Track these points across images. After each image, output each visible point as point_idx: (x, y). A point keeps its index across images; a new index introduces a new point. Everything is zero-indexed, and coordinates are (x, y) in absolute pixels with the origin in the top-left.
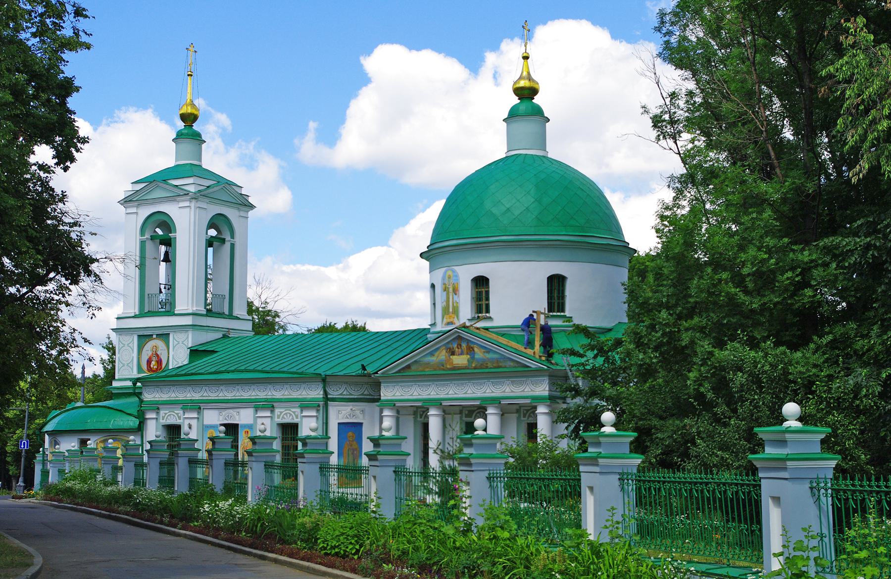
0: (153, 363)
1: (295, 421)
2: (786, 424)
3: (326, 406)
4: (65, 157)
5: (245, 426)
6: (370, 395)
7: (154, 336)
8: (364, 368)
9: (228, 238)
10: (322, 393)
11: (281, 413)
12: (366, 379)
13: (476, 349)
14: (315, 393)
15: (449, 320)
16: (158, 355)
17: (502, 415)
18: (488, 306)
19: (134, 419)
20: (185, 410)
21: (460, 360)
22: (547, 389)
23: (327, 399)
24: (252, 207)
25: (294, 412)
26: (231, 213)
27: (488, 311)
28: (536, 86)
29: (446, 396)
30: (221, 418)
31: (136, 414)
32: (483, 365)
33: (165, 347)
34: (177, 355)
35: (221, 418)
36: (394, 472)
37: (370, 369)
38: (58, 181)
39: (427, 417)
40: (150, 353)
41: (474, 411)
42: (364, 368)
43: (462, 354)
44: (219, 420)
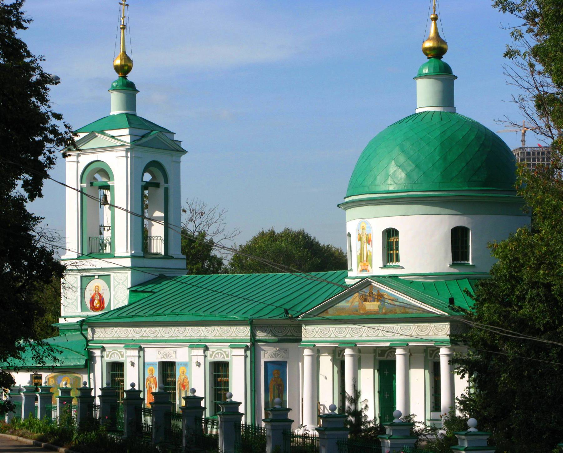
0: (96, 302)
1: (226, 359)
2: (469, 430)
4: (34, 190)
5: (181, 364)
7: (96, 277)
9: (162, 182)
11: (213, 352)
12: (289, 322)
15: (363, 268)
17: (411, 355)
18: (397, 255)
20: (126, 347)
21: (372, 306)
23: (254, 340)
24: (184, 152)
25: (225, 352)
26: (164, 158)
27: (398, 260)
28: (444, 46)
29: (360, 339)
30: (160, 356)
33: (107, 287)
34: (118, 293)
35: (160, 356)
36: (283, 433)
38: (31, 207)
39: (344, 356)
40: (93, 293)
41: (387, 350)
42: (286, 311)
44: (158, 358)
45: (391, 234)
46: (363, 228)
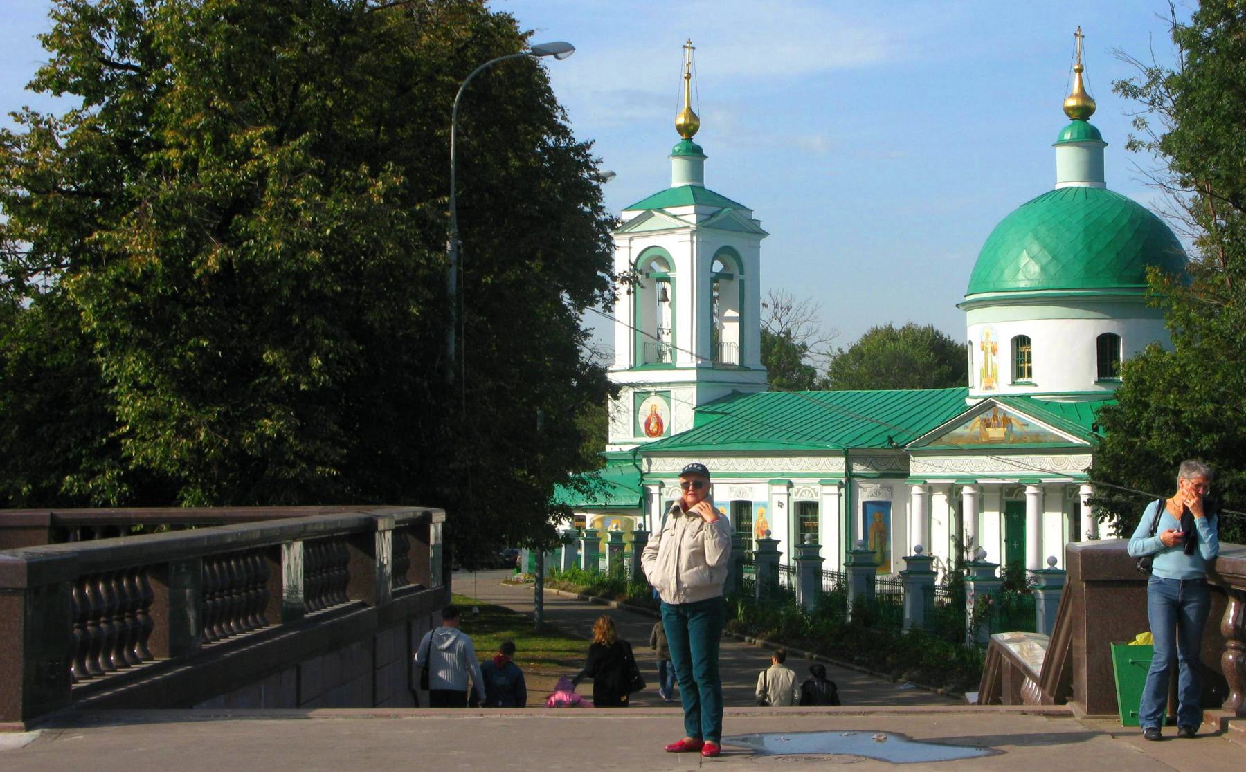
0: (653, 425)
1: (815, 499)
8: (890, 440)
12: (893, 452)
16: (657, 416)
18: (1030, 369)
23: (850, 475)
27: (1030, 375)
37: (896, 441)
40: (649, 413)
42: (890, 440)
43: (999, 426)
45: (1021, 342)
46: (987, 335)
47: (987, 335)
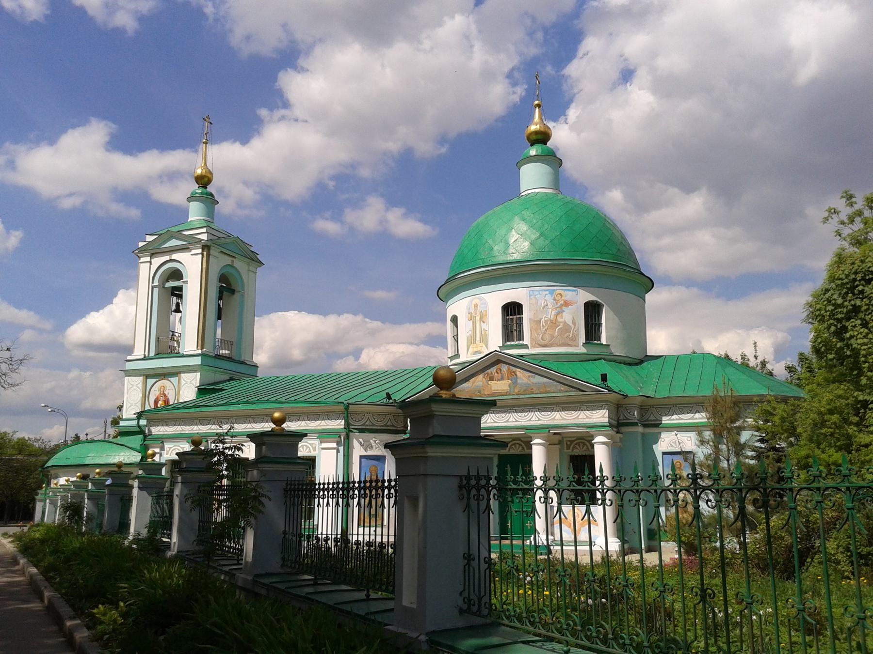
1: (312, 454)
3: (348, 437)
6: (393, 426)
10: (343, 422)
13: (518, 373)
14: (338, 424)
19: (136, 453)
22: (607, 415)
25: (311, 444)
31: (138, 448)
32: (528, 389)
43: (502, 379)
46: (476, 306)
47: (476, 306)
